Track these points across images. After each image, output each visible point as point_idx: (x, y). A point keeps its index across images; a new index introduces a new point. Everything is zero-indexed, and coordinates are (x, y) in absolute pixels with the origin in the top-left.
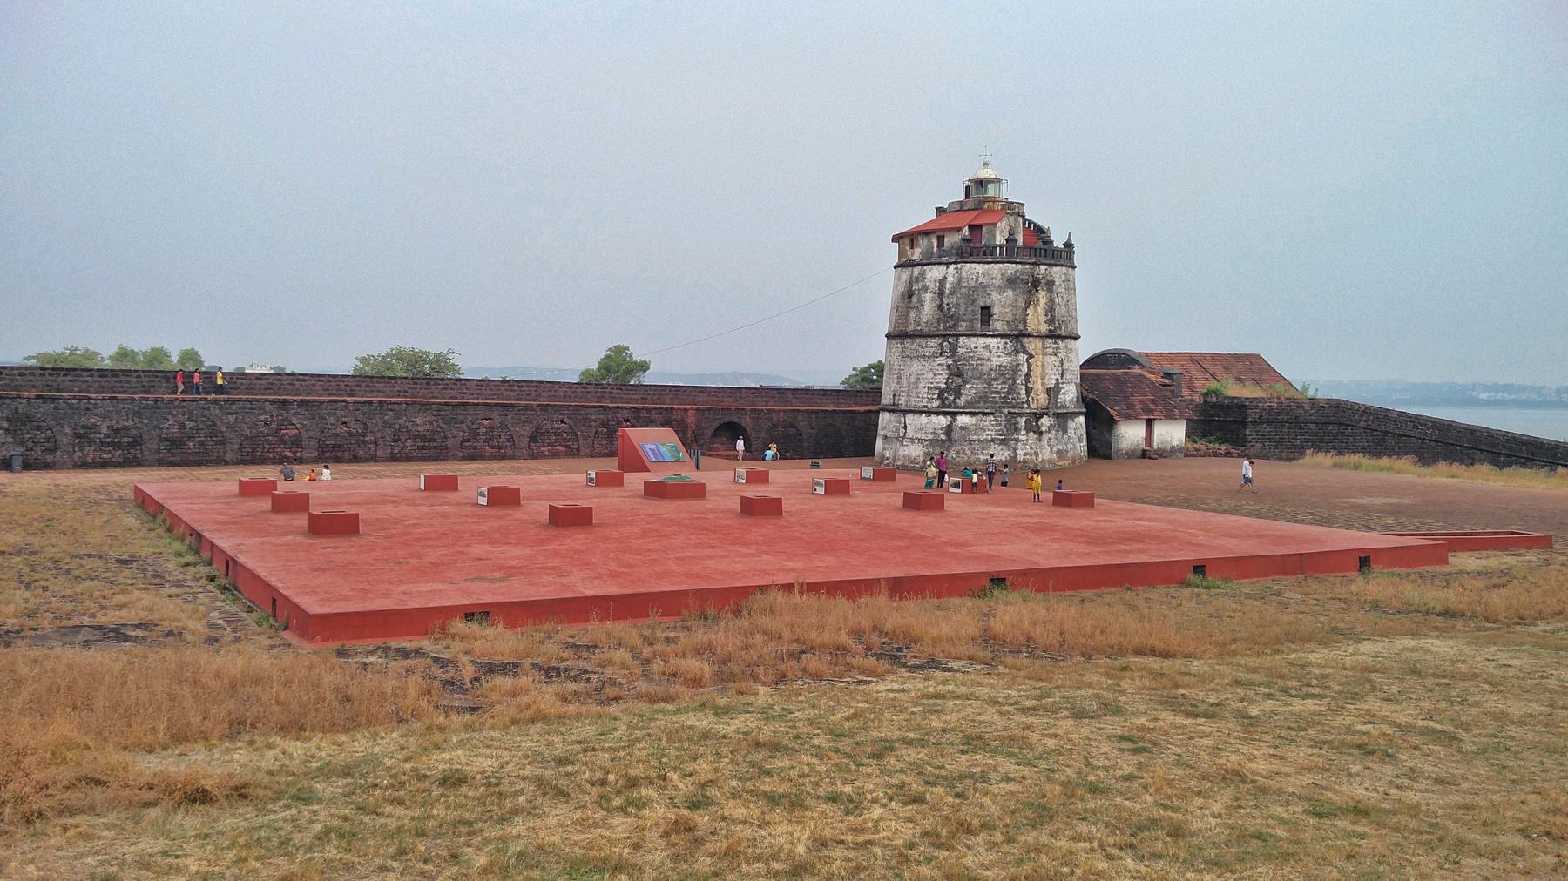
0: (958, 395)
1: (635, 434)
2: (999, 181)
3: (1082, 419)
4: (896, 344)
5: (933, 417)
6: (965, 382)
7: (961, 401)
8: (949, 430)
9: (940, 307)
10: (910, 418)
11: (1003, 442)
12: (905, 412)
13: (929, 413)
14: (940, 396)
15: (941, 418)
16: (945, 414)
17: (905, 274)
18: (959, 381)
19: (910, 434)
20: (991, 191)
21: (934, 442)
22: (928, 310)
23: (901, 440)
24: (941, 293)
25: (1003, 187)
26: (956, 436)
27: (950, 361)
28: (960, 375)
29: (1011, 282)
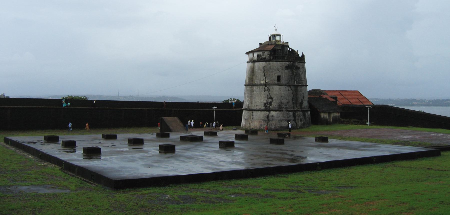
1: (167, 119)
2: (280, 35)
3: (309, 112)
4: (248, 87)
5: (263, 112)
6: (273, 101)
8: (268, 117)
10: (255, 113)
11: (286, 120)
15: (265, 112)
16: (267, 111)
17: (251, 64)
18: (270, 100)
20: (277, 38)
25: (282, 37)
26: (270, 118)
28: (271, 98)
29: (287, 68)
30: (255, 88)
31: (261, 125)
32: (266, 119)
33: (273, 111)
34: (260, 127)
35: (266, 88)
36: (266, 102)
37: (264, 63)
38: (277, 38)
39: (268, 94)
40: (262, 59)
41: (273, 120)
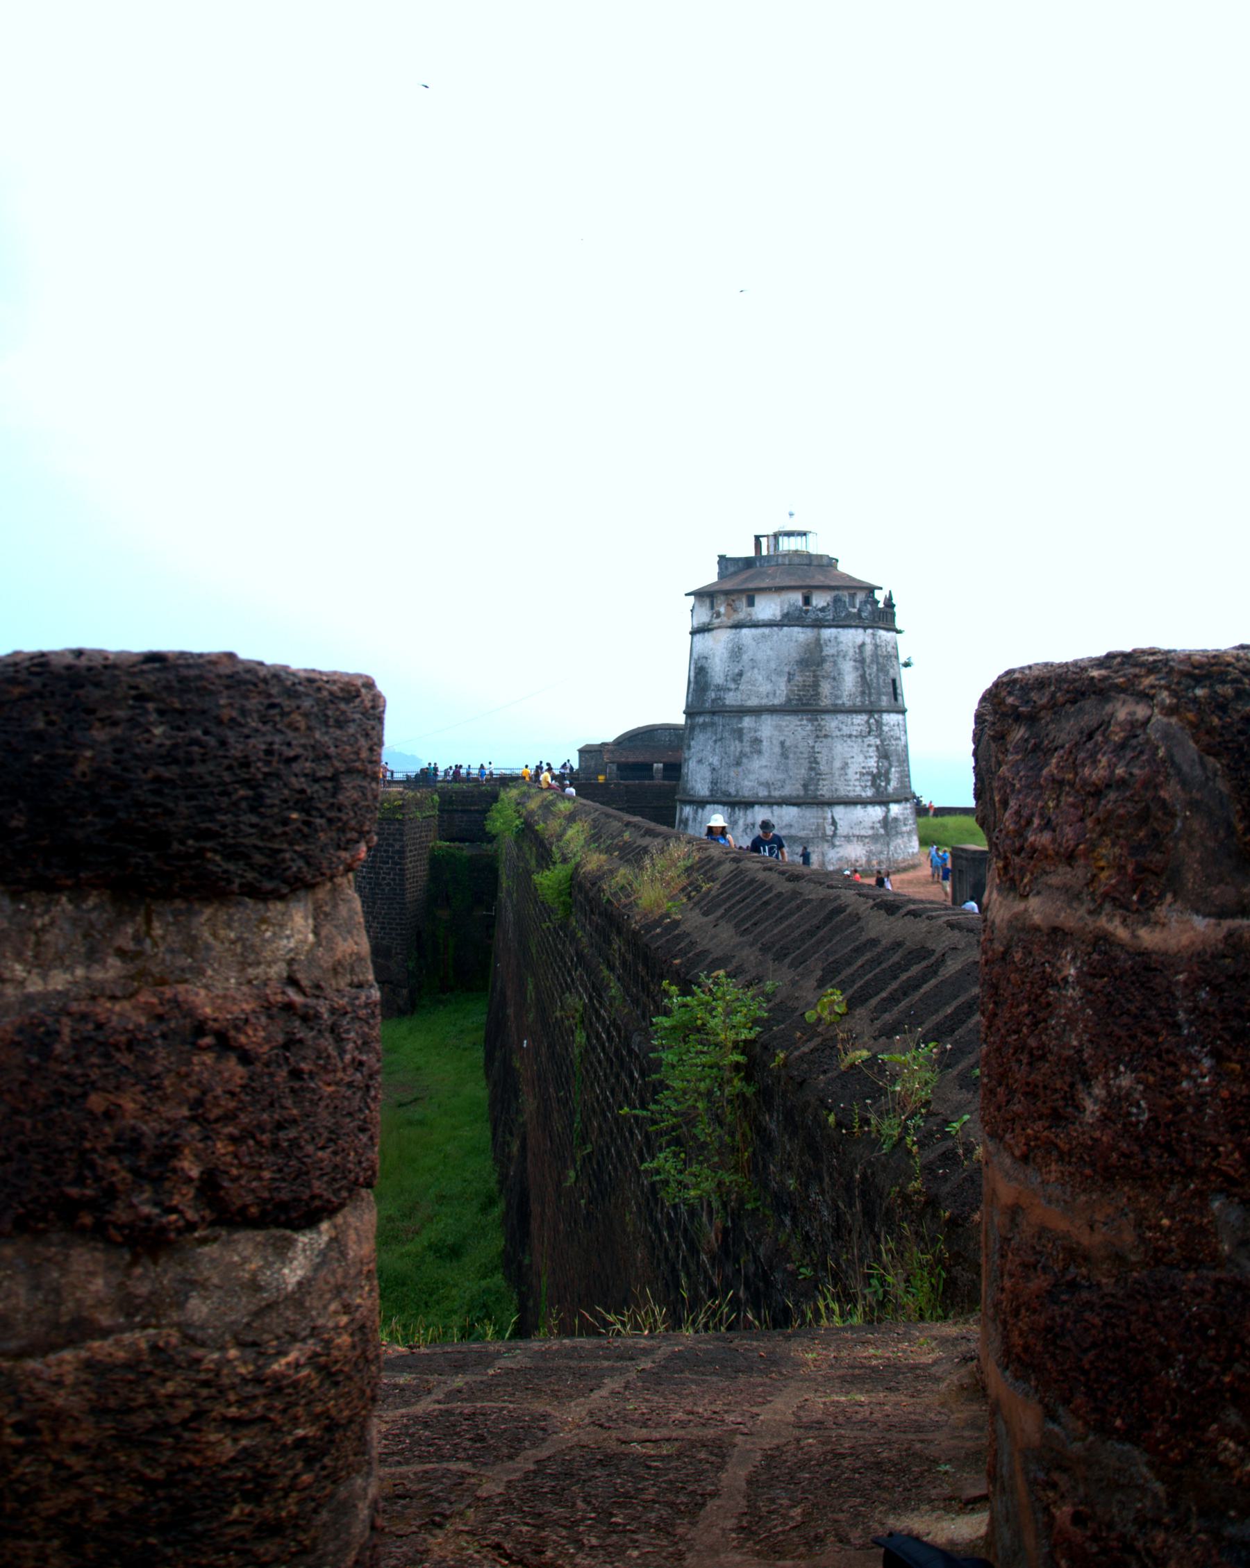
0: (888, 781)
5: (870, 809)
6: (891, 766)
7: (890, 789)
9: (863, 677)
10: (839, 812)
12: (831, 803)
13: (864, 803)
14: (874, 784)
16: (881, 803)
17: (801, 635)
19: (842, 830)
21: (875, 838)
22: (850, 680)
23: (831, 840)
24: (862, 661)
27: (878, 743)
30: (832, 723)
31: (870, 851)
32: (882, 831)
33: (897, 802)
34: (869, 861)
35: (872, 721)
36: (875, 771)
37: (860, 631)
38: (787, 545)
39: (878, 743)
40: (849, 615)
41: (897, 833)
